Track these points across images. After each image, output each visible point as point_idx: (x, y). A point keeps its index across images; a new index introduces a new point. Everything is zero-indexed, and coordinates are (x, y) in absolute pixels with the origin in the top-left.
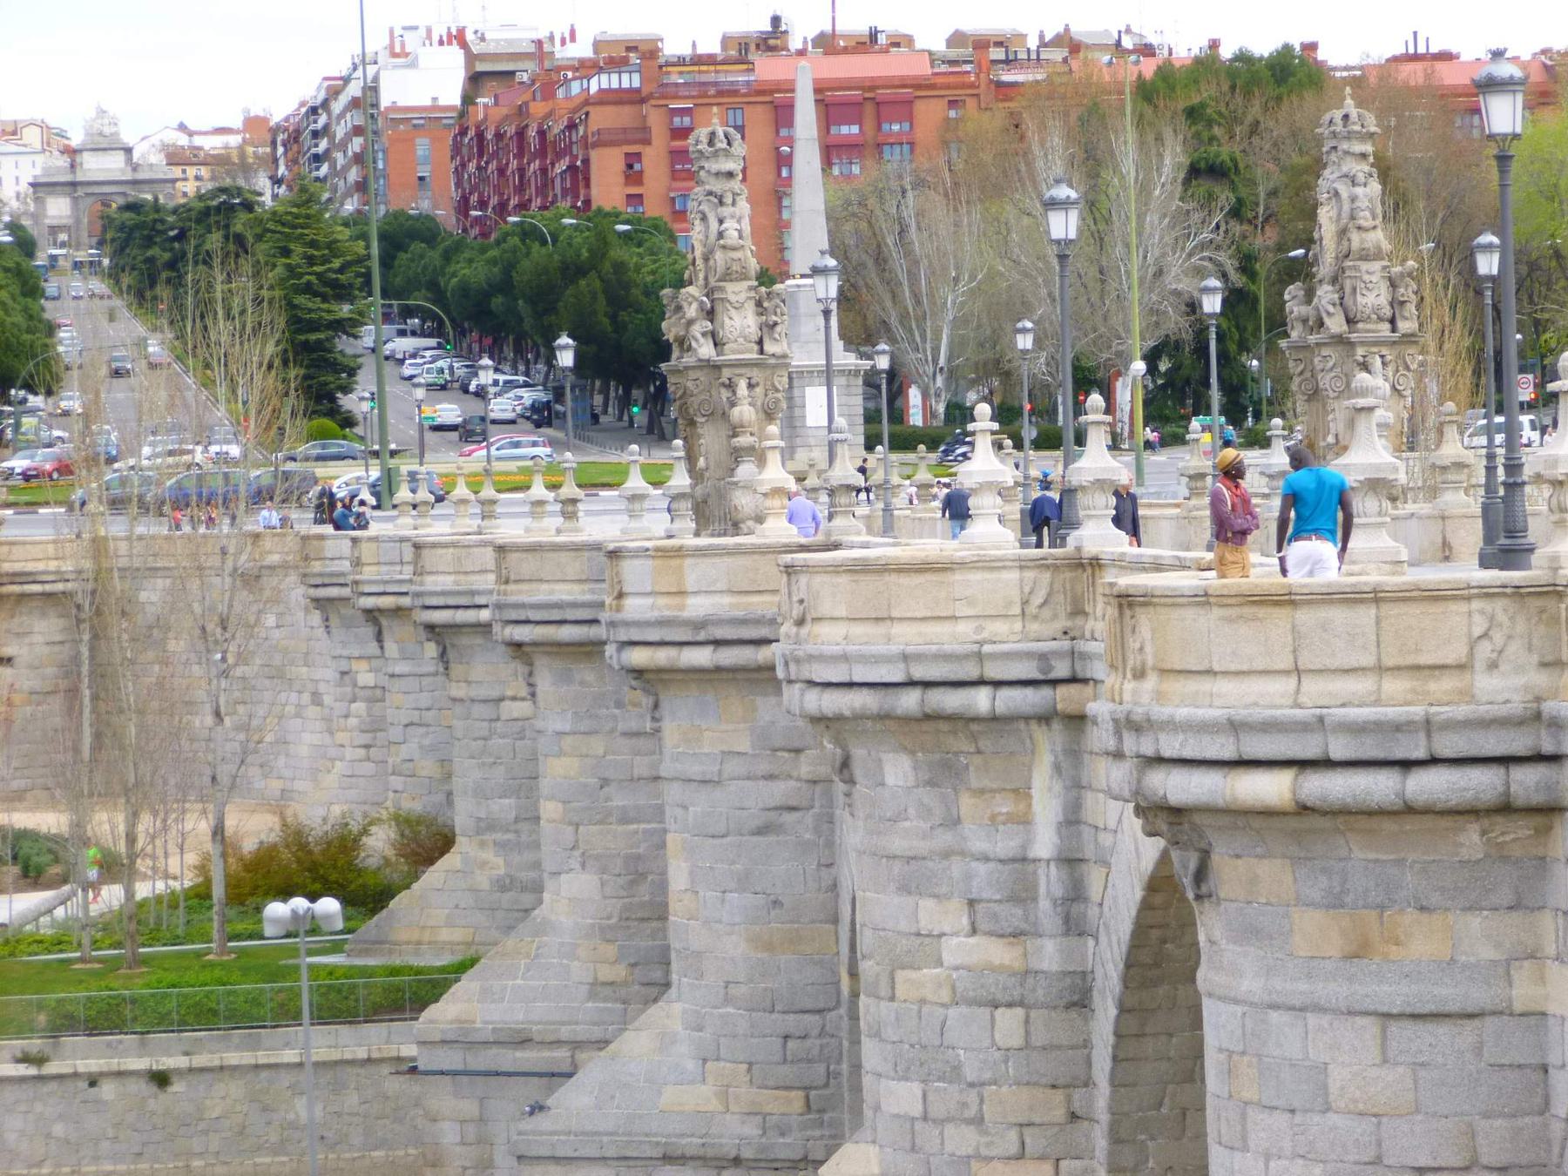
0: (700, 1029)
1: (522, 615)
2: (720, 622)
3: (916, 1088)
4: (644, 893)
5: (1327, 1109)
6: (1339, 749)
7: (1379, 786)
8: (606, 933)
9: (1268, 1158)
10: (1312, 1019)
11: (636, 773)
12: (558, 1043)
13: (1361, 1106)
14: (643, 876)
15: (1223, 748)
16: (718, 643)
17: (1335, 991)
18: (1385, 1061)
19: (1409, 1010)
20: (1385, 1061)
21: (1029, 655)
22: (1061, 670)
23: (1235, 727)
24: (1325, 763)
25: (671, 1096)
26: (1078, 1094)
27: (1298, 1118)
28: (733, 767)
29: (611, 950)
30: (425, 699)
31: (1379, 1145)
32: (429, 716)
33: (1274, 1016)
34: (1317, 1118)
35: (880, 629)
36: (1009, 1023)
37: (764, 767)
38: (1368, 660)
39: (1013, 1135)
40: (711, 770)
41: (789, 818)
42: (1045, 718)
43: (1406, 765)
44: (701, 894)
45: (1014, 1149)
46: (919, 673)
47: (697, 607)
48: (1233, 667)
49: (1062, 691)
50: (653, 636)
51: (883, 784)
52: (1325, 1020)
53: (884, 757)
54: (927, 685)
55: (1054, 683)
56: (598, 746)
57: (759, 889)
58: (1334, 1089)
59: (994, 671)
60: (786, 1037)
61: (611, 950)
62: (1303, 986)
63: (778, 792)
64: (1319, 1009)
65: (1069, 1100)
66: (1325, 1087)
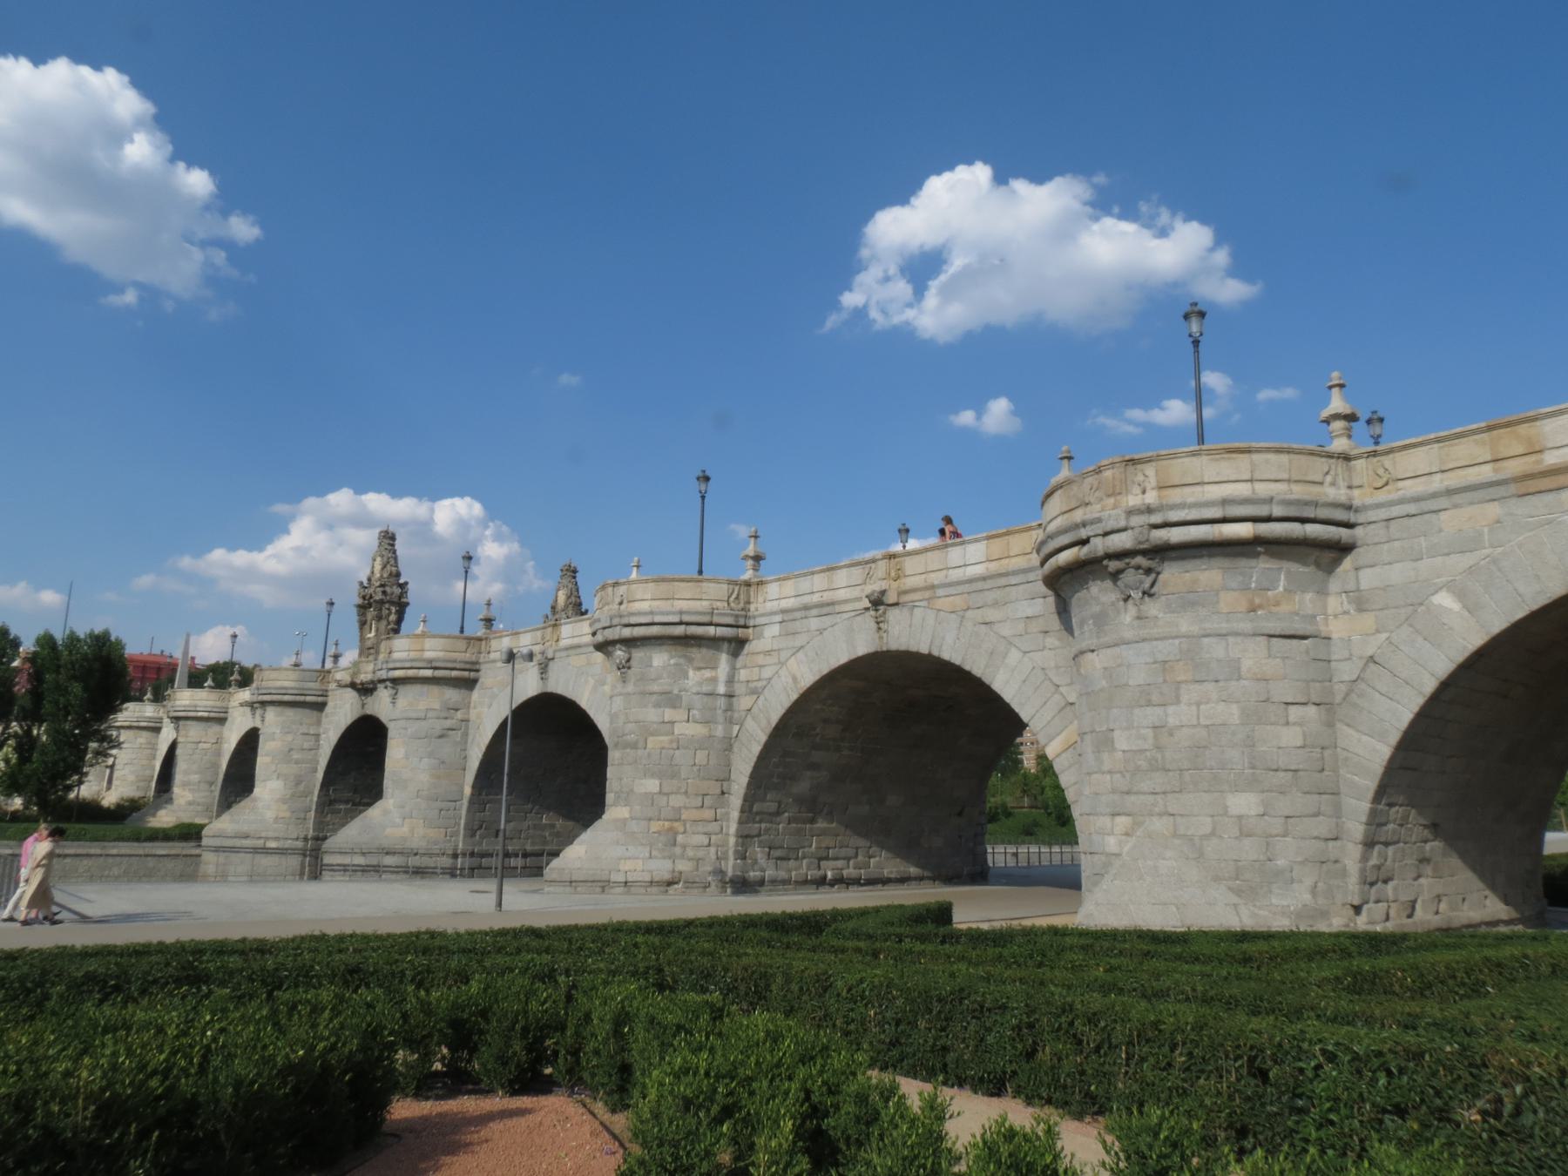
0: (403, 807)
1: (269, 691)
3: (657, 782)
4: (301, 788)
5: (1239, 678)
6: (1277, 511)
7: (1294, 529)
8: (284, 801)
9: (1198, 704)
10: (1231, 639)
11: (305, 747)
12: (260, 838)
13: (1259, 676)
14: (302, 782)
15: (1216, 513)
17: (1246, 626)
18: (1270, 656)
19: (1283, 633)
20: (1270, 656)
21: (732, 615)
22: (742, 622)
23: (1225, 502)
24: (1269, 519)
25: (389, 831)
26: (725, 784)
27: (1221, 684)
28: (430, 714)
29: (285, 807)
30: (134, 756)
31: (1268, 692)
32: (135, 761)
33: (1206, 640)
34: (1233, 683)
35: (670, 602)
36: (701, 757)
37: (444, 714)
38: (1285, 476)
39: (700, 799)
40: (423, 715)
41: (450, 732)
42: (729, 640)
43: (1303, 521)
45: (700, 804)
46: (686, 618)
47: (429, 655)
48: (1217, 480)
49: (740, 630)
50: (408, 665)
51: (651, 666)
52: (1239, 639)
53: (654, 655)
54: (688, 624)
55: (738, 627)
56: (289, 738)
58: (1244, 669)
59: (716, 619)
60: (441, 810)
61: (285, 807)
62: (1224, 625)
63: (448, 723)
64: (1236, 634)
65: (722, 786)
66: (1239, 668)
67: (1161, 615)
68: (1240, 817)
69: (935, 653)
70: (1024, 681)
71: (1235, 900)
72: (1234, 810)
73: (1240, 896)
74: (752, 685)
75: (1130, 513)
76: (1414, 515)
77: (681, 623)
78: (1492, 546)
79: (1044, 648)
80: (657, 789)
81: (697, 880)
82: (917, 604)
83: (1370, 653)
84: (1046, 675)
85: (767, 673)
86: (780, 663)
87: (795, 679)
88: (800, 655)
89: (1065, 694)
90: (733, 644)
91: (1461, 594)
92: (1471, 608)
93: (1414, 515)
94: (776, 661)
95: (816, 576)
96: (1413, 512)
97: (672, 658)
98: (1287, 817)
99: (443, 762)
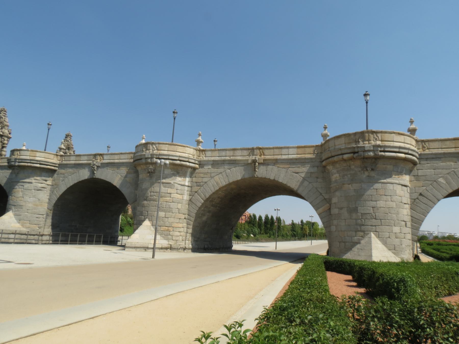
2: (42, 161)
16: (40, 164)
44: (25, 198)
46: (181, 159)
54: (180, 161)
57: (37, 197)
63: (43, 185)
67: (375, 176)
68: (395, 233)
69: (276, 179)
70: (310, 191)
71: (394, 256)
72: (394, 231)
73: (395, 254)
74: (198, 184)
75: (374, 146)
76: (434, 158)
77: (179, 160)
78: (454, 168)
79: (317, 182)
80: (164, 216)
81: (176, 247)
82: (269, 164)
83: (420, 192)
84: (317, 190)
85: (205, 180)
86: (211, 177)
87: (217, 183)
88: (220, 175)
89: (324, 196)
90: (192, 169)
91: (446, 179)
92: (448, 183)
93: (434, 158)
94: (210, 176)
95: (227, 151)
96: (434, 157)
97: (172, 171)
98: (405, 234)
99: (39, 200)
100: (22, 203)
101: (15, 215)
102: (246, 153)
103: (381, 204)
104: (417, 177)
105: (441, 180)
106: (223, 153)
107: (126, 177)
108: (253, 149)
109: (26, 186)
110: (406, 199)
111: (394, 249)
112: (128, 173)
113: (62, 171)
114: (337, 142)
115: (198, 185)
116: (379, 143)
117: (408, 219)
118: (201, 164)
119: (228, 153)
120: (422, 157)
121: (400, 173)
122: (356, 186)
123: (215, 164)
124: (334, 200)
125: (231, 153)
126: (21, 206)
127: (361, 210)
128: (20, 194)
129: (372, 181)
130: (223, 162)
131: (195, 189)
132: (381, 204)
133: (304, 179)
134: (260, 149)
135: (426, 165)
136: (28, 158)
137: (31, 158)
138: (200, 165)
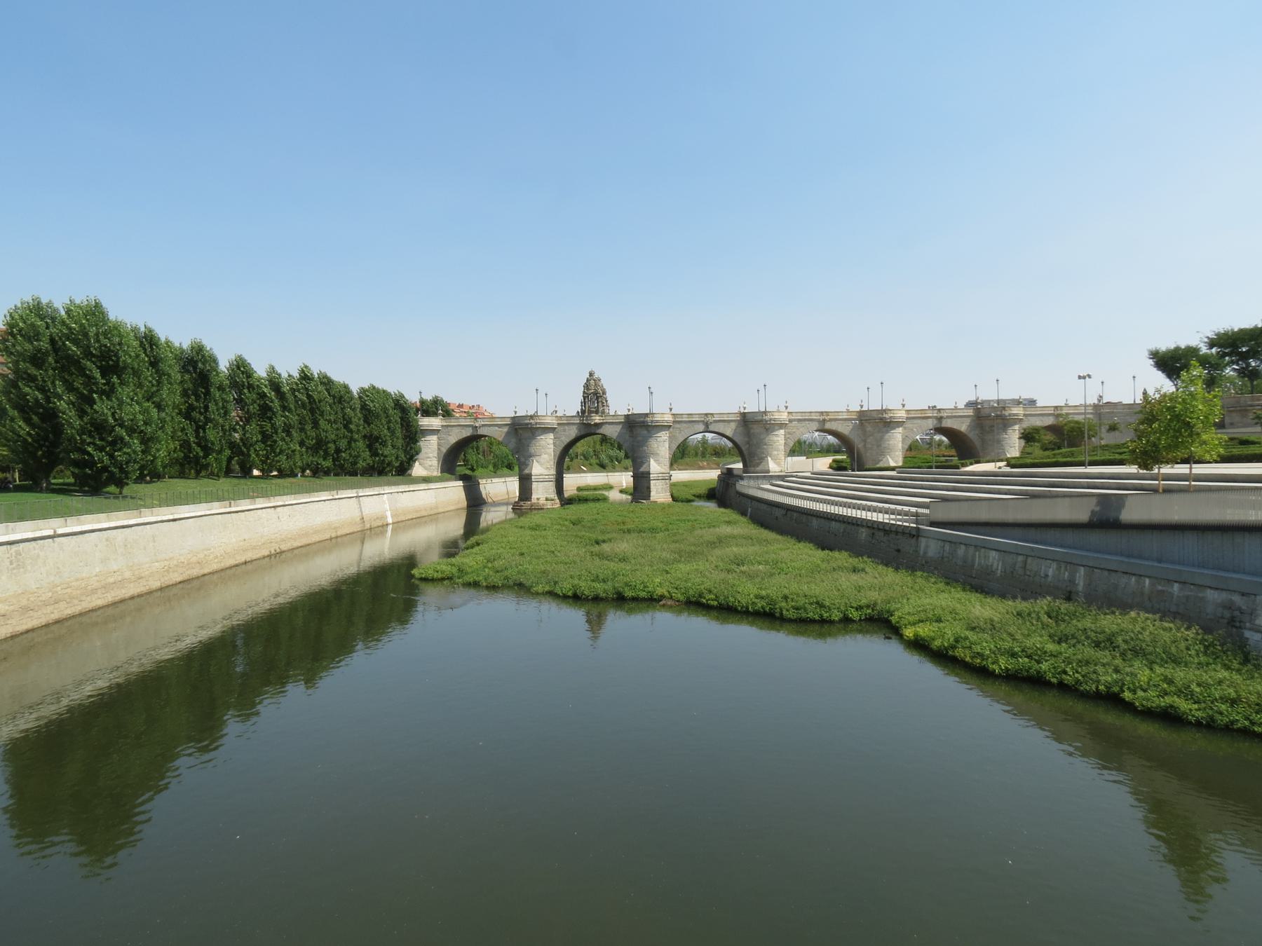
85: (794, 431)
100: (658, 452)
101: (655, 460)
102: (818, 414)
103: (891, 442)
104: (905, 428)
105: (915, 430)
106: (803, 414)
107: (735, 429)
108: (822, 412)
109: (659, 439)
110: (901, 440)
111: (896, 462)
112: (737, 427)
113: (678, 426)
114: (872, 412)
115: (789, 433)
116: (892, 415)
117: (901, 448)
118: (790, 421)
119: (807, 414)
120: (907, 418)
121: (899, 427)
122: (880, 434)
123: (799, 420)
124: (868, 441)
125: (809, 414)
126: (657, 454)
127: (883, 446)
128: (656, 445)
129: (887, 432)
130: (805, 420)
131: (788, 436)
132: (891, 442)
133: (852, 430)
134: (826, 412)
135: (909, 421)
136: (659, 419)
137: (662, 419)
138: (789, 421)
